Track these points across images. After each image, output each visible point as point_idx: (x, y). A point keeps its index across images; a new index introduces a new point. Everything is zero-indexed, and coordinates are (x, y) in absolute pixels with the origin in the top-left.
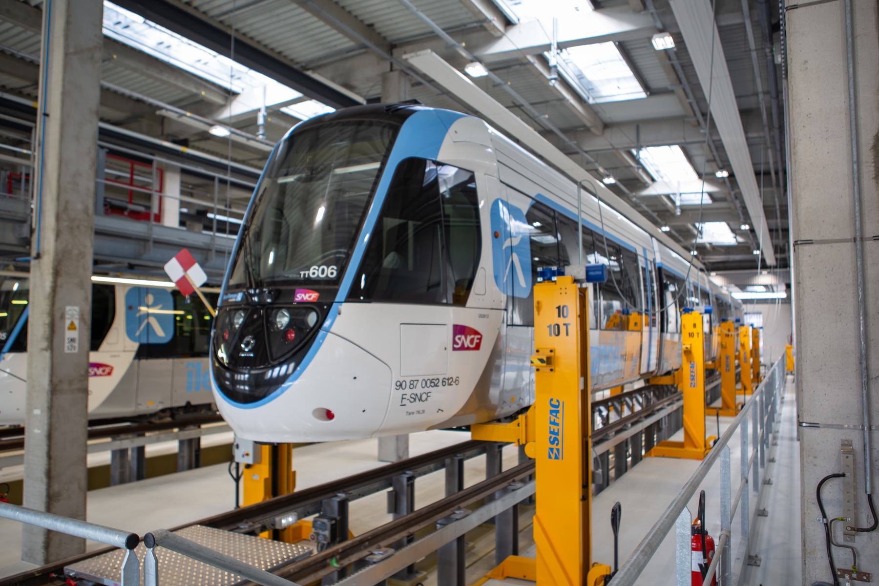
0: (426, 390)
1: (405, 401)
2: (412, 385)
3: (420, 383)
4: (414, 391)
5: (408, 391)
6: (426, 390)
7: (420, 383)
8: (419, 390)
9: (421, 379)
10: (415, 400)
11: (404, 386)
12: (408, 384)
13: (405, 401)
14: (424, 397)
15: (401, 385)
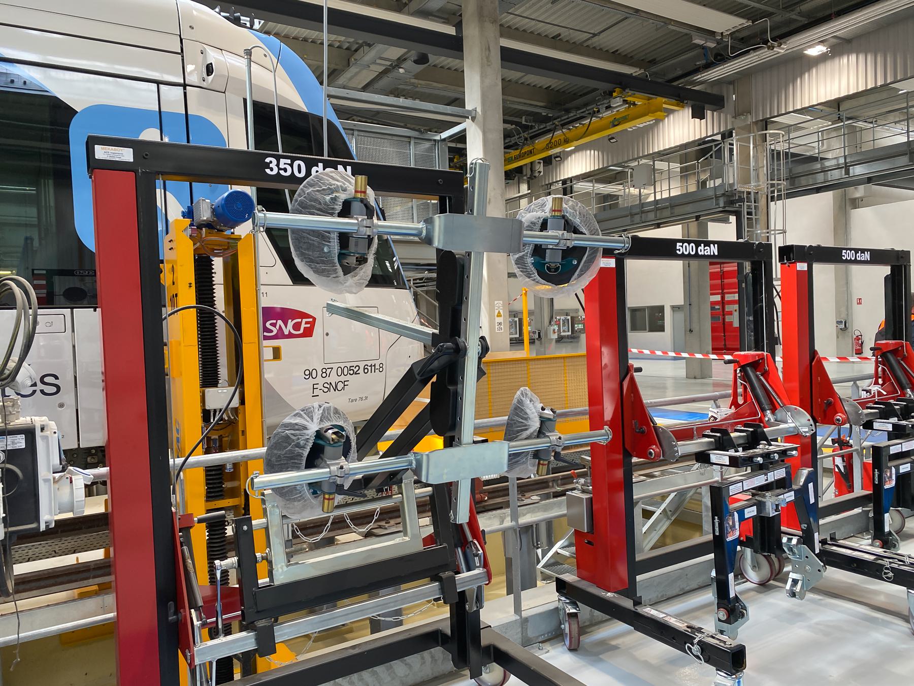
0: (343, 378)
1: (316, 392)
2: (325, 373)
3: (334, 371)
4: (328, 380)
5: (320, 380)
6: (343, 378)
7: (334, 371)
8: (333, 379)
9: (335, 366)
10: (329, 390)
11: (314, 375)
12: (320, 373)
13: (316, 392)
14: (340, 386)
15: (310, 374)
